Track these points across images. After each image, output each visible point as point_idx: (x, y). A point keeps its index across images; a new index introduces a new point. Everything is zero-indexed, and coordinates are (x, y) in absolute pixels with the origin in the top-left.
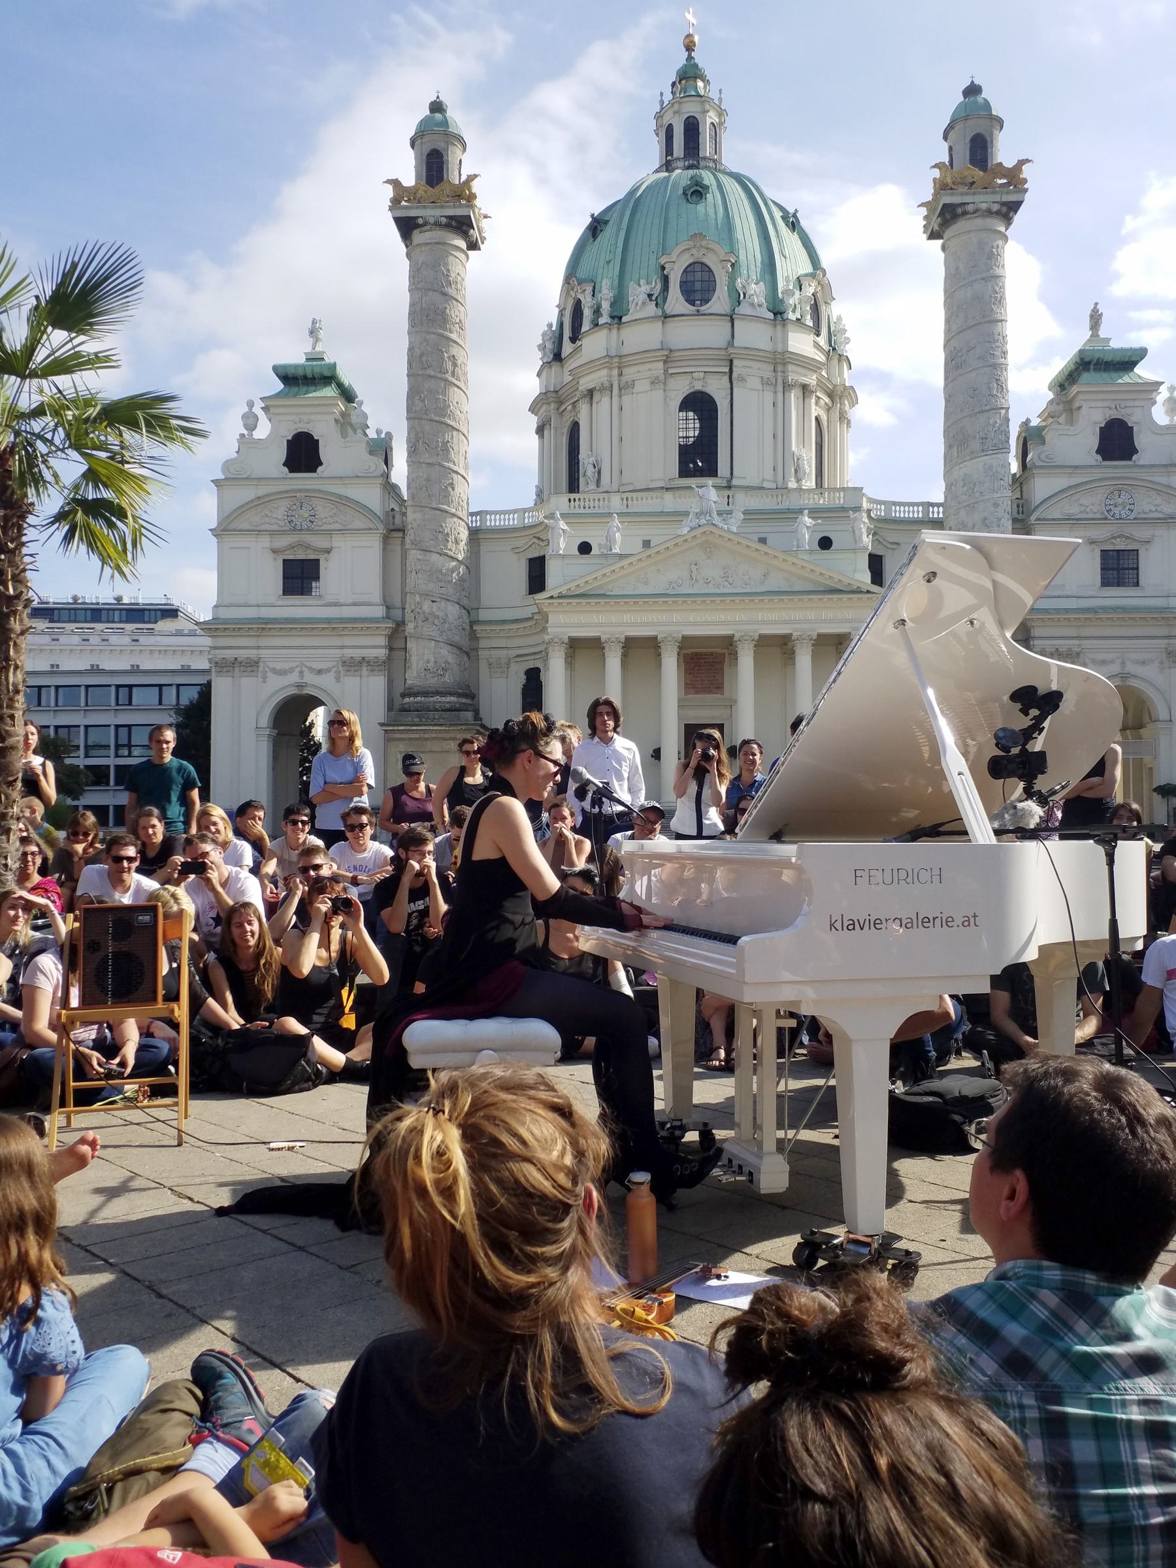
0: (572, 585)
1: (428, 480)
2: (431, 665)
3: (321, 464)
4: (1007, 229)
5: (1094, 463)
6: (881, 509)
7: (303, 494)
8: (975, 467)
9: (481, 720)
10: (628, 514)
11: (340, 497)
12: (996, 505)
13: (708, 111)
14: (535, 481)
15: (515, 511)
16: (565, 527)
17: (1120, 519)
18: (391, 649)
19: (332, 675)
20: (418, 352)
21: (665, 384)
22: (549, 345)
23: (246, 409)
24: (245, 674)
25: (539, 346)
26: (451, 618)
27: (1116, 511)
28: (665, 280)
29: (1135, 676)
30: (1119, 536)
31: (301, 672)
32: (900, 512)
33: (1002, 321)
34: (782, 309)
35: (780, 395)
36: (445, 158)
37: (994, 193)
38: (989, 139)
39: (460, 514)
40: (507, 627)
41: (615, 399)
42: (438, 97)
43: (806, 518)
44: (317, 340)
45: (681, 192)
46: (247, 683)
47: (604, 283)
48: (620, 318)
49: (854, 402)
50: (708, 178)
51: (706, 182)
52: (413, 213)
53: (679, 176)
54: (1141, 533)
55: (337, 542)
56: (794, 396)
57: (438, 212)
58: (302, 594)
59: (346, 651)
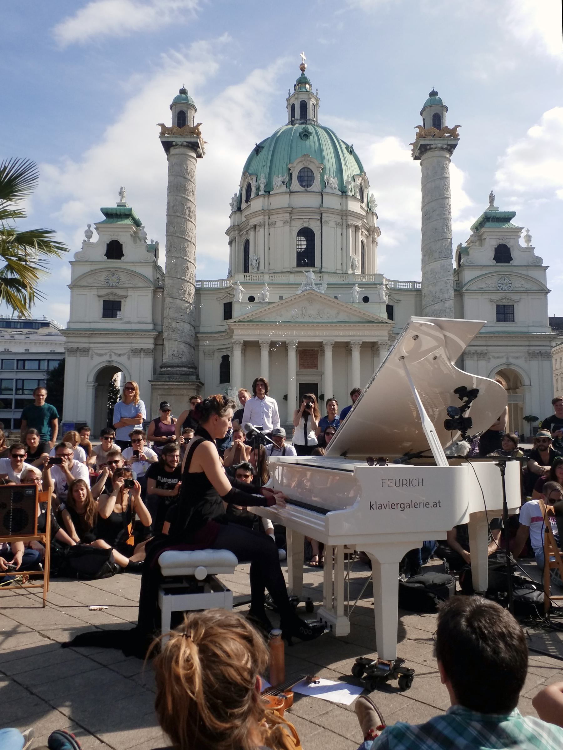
0: (245, 316)
1: (176, 265)
2: (175, 353)
3: (123, 255)
4: (450, 156)
5: (493, 264)
6: (392, 285)
7: (114, 270)
8: (436, 265)
9: (200, 380)
10: (272, 284)
11: (132, 271)
13: (311, 99)
14: (228, 266)
15: (218, 281)
17: (505, 290)
18: (156, 344)
19: (125, 357)
20: (172, 204)
21: (290, 223)
22: (235, 204)
23: (87, 228)
24: (82, 355)
25: (230, 204)
26: (186, 330)
27: (503, 287)
28: (291, 175)
29: (514, 364)
30: (505, 298)
31: (110, 355)
33: (448, 198)
34: (345, 190)
35: (344, 230)
36: (186, 115)
37: (444, 140)
39: (191, 281)
40: (213, 335)
41: (267, 230)
42: (184, 87)
44: (123, 197)
45: (298, 134)
46: (83, 359)
47: (262, 175)
48: (269, 192)
49: (379, 234)
50: (311, 129)
51: (310, 131)
52: (170, 140)
53: (298, 127)
54: (515, 297)
55: (130, 293)
56: (351, 231)
57: (183, 140)
58: (112, 317)
59: (133, 345)
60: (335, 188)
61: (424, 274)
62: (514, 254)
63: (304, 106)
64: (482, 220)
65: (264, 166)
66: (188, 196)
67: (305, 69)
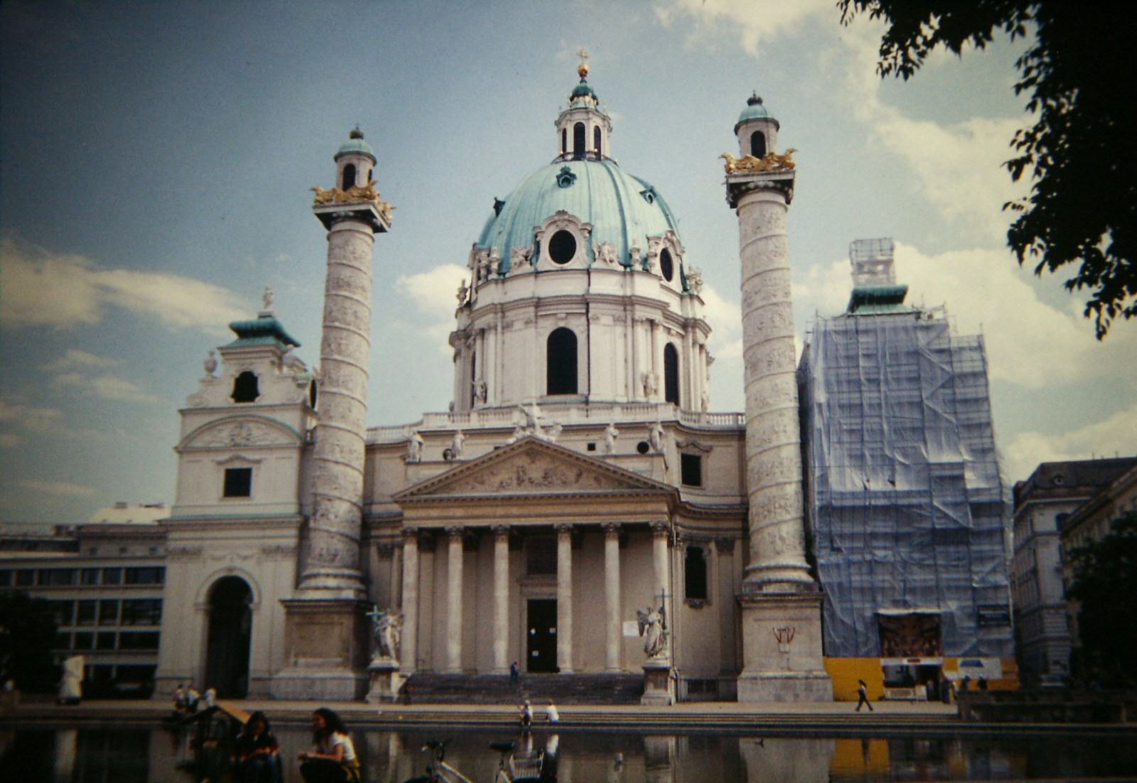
2: (324, 552)
7: (243, 419)
15: (403, 427)
21: (536, 322)
28: (538, 244)
31: (232, 560)
35: (630, 329)
36: (357, 169)
41: (499, 336)
43: (612, 430)
48: (504, 274)
49: (707, 330)
60: (611, 261)
61: (748, 399)
63: (580, 130)
65: (500, 233)
66: (354, 293)
67: (586, 72)
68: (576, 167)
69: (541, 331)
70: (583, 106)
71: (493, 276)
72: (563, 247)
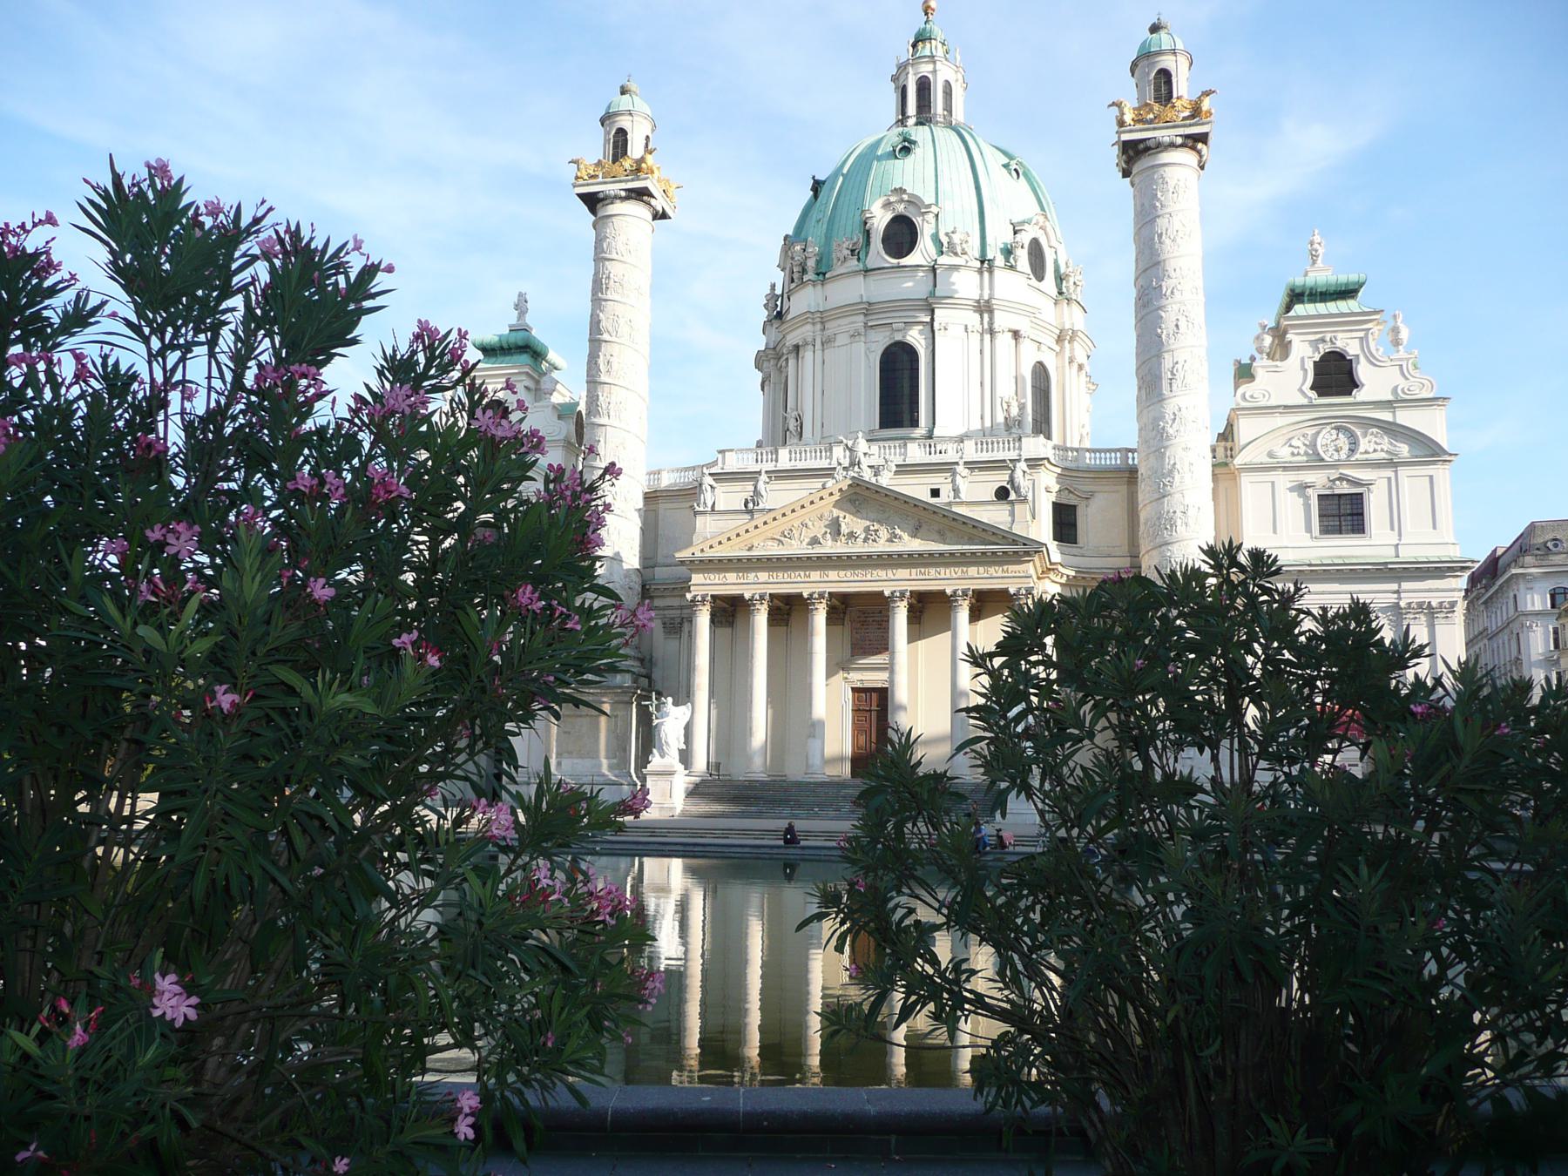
5: (1305, 401)
12: (1186, 449)
16: (713, 483)
25: (765, 305)
28: (867, 234)
32: (1111, 459)
36: (629, 137)
38: (1173, 74)
48: (824, 274)
56: (1004, 341)
62: (1363, 371)
63: (924, 86)
64: (1288, 299)
65: (818, 221)
68: (920, 134)
69: (873, 347)
70: (929, 54)
71: (810, 276)
72: (902, 235)
